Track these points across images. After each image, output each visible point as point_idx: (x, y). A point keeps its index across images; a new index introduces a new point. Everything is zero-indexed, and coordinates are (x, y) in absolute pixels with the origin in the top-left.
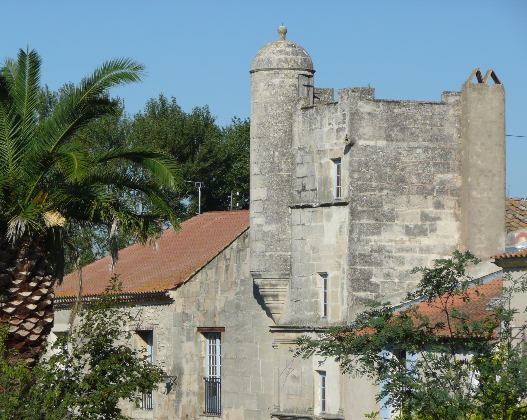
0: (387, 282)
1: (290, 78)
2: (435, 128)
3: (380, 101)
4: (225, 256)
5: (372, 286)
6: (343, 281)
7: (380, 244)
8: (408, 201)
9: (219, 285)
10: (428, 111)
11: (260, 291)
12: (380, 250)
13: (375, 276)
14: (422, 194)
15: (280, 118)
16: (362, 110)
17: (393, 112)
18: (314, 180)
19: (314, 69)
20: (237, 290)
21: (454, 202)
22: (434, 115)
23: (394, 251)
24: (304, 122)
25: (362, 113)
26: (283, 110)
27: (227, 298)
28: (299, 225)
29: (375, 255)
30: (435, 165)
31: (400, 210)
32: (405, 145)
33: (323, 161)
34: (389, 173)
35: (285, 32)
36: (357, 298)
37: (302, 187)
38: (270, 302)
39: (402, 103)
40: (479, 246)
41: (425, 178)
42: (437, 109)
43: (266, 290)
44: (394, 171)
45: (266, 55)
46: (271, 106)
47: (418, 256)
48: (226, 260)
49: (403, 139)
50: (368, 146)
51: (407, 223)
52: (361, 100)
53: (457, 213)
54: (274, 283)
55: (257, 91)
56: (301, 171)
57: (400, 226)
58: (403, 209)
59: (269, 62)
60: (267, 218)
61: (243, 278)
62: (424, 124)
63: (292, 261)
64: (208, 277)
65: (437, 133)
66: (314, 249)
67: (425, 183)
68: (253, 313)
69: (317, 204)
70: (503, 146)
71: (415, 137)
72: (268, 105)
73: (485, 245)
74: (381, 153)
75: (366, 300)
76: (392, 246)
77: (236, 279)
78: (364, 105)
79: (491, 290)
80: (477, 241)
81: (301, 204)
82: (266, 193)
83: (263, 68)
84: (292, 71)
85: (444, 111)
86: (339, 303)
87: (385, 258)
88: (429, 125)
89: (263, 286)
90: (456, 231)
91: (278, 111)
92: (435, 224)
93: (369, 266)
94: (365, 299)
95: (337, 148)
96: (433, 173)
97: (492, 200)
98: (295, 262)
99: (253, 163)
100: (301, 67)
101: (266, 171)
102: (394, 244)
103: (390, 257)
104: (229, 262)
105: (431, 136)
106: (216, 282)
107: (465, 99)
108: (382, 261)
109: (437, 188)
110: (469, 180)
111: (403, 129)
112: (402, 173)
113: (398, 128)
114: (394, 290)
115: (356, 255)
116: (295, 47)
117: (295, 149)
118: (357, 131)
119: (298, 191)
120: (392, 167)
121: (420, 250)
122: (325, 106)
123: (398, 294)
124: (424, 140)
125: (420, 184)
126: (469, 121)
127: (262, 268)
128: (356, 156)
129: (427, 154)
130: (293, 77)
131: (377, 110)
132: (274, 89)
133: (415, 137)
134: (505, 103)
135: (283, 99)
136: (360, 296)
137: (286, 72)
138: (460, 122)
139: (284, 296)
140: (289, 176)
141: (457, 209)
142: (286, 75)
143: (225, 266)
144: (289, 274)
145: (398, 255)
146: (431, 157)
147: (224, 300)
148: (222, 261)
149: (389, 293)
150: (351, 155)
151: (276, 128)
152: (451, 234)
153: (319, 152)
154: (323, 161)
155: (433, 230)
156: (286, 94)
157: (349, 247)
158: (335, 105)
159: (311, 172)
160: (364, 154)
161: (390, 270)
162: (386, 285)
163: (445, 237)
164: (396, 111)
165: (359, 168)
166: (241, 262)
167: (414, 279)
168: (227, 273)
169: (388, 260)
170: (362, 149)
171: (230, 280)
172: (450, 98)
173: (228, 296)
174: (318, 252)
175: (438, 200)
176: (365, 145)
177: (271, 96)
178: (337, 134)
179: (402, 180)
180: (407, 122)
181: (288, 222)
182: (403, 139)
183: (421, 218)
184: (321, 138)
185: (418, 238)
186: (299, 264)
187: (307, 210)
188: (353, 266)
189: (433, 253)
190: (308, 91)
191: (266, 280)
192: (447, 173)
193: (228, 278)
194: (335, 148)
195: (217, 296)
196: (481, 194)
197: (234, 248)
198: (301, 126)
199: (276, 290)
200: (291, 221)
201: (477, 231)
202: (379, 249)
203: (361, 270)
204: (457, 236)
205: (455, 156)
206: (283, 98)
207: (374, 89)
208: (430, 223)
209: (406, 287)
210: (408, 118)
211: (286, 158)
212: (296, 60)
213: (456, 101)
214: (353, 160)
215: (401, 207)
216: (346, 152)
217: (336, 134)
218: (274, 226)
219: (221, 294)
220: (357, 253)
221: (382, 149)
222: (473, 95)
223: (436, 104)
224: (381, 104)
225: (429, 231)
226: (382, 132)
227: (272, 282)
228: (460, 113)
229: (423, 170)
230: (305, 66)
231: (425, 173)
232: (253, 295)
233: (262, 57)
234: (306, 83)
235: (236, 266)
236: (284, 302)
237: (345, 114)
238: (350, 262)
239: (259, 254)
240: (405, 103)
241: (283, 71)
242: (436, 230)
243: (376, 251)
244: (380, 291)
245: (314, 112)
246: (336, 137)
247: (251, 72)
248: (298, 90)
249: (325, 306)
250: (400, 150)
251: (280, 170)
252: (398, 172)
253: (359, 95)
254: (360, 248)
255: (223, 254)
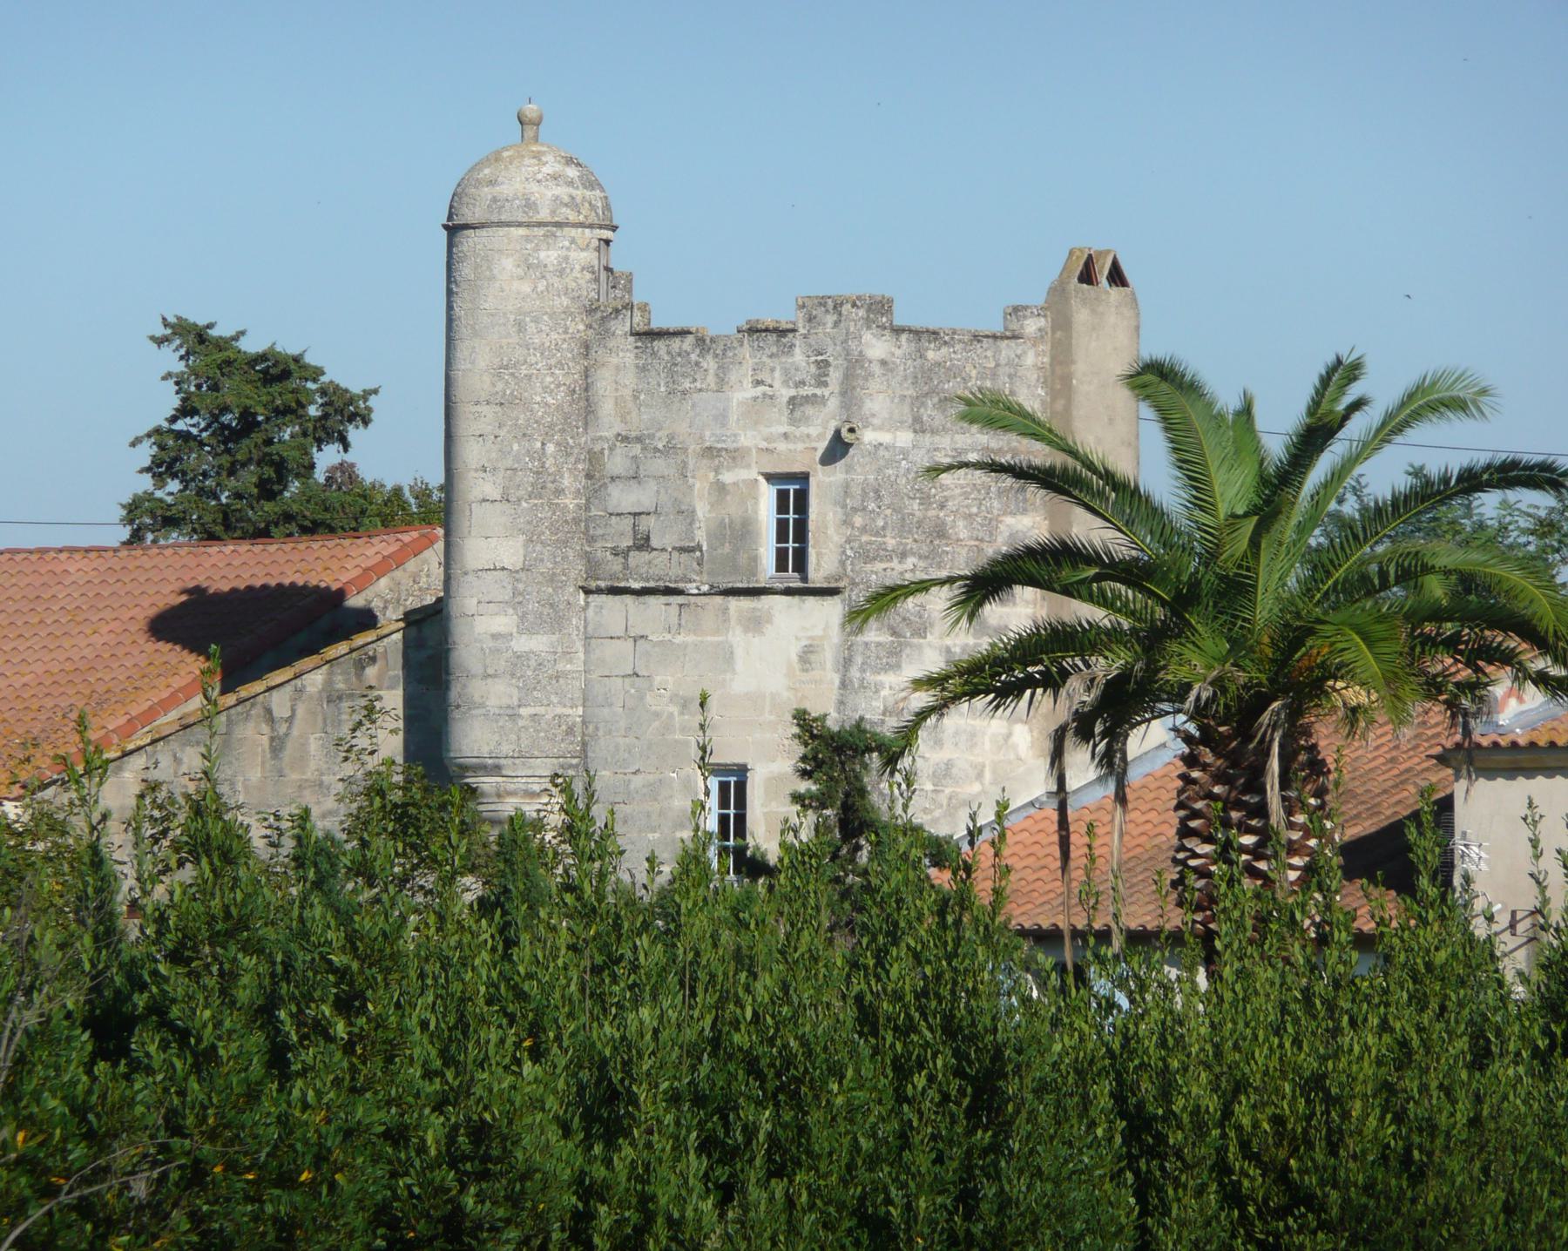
24: (643, 369)
26: (566, 332)
34: (918, 513)
46: (536, 320)
52: (869, 328)
59: (529, 205)
60: (523, 618)
67: (982, 540)
77: (322, 774)
78: (874, 341)
82: (521, 551)
89: (499, 796)
91: (554, 336)
98: (600, 733)
101: (521, 493)
113: (936, 400)
127: (506, 749)
131: (898, 352)
137: (573, 232)
142: (573, 241)
151: (549, 379)
153: (709, 452)
154: (727, 477)
164: (931, 355)
171: (295, 776)
187: (655, 602)
194: (782, 446)
198: (629, 379)
206: (565, 301)
209: (945, 803)
211: (572, 459)
218: (545, 638)
221: (905, 453)
224: (904, 337)
241: (566, 230)
251: (559, 492)
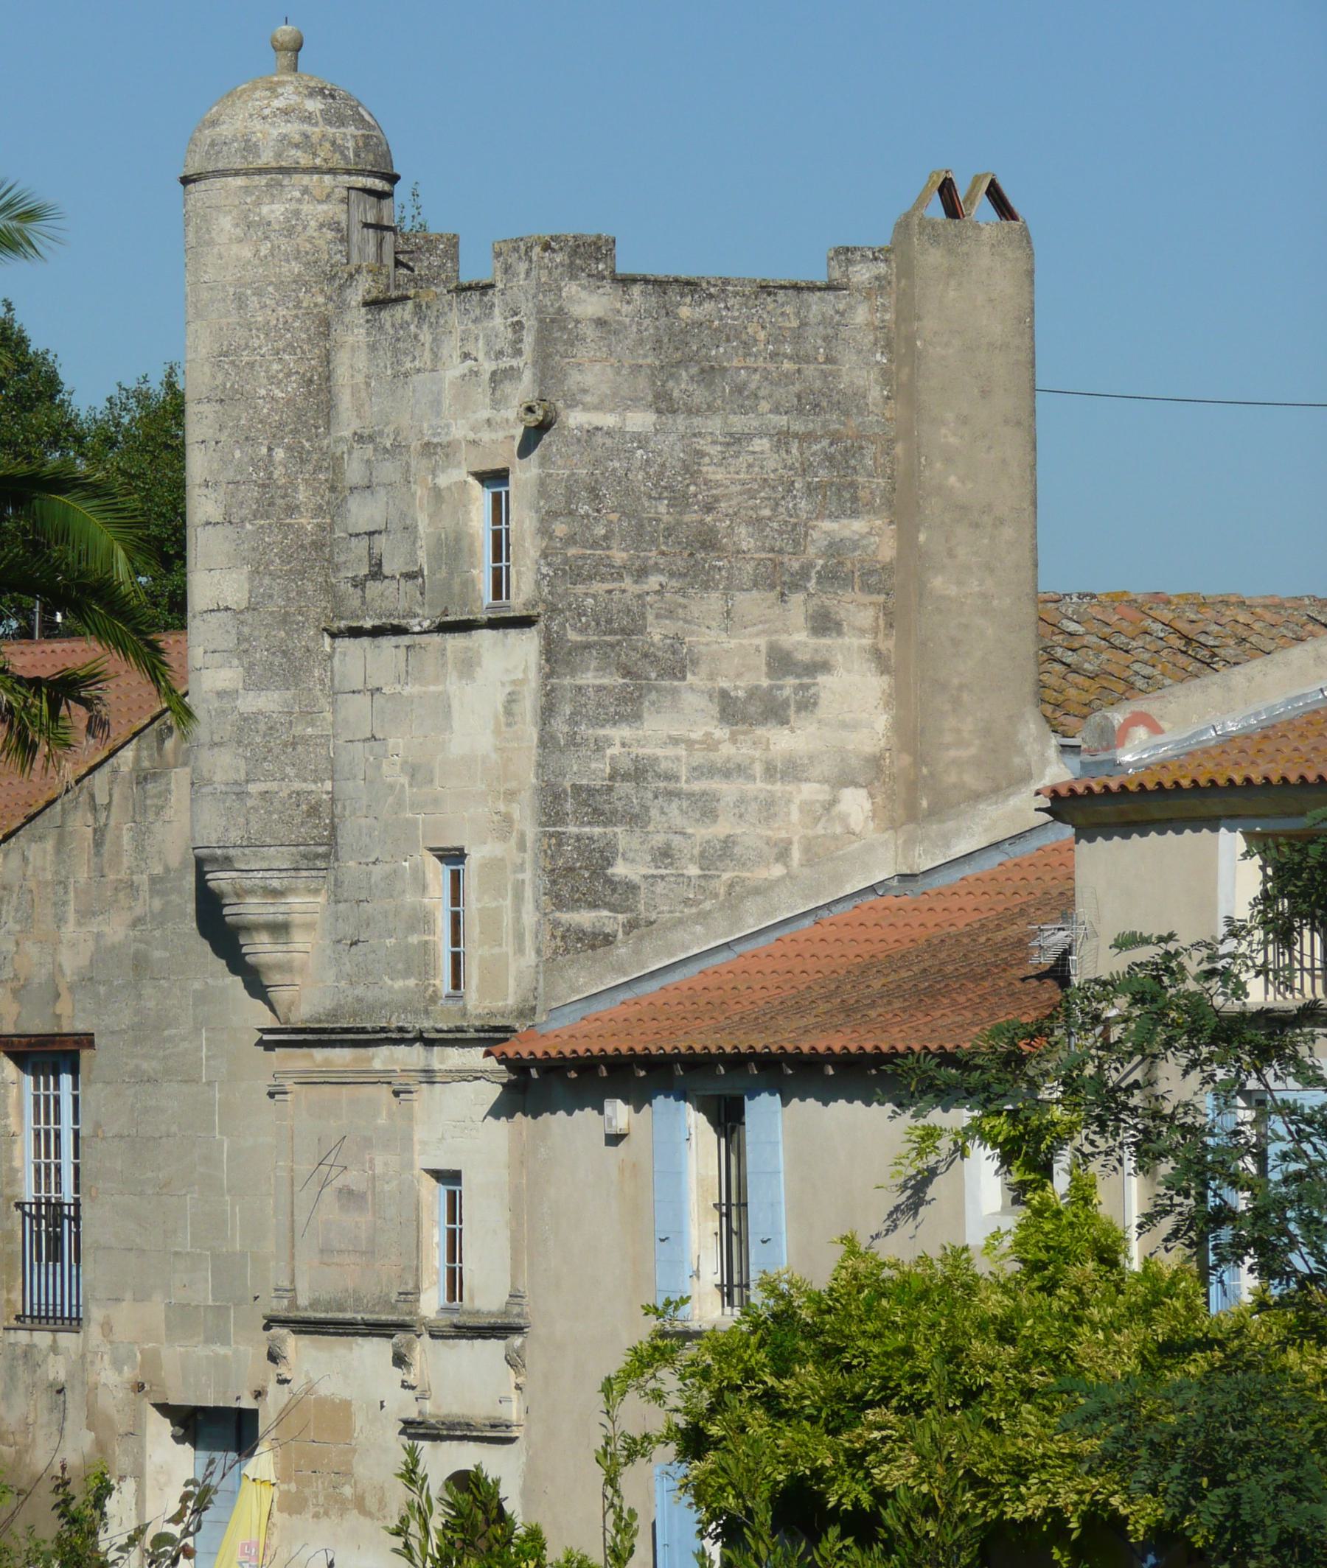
0: (662, 877)
1: (320, 202)
2: (810, 370)
3: (634, 280)
4: (92, 797)
5: (614, 890)
6: (520, 876)
7: (641, 751)
8: (728, 612)
9: (72, 894)
10: (786, 311)
11: (226, 911)
12: (639, 772)
13: (625, 859)
14: (772, 587)
15: (289, 335)
16: (576, 310)
17: (676, 317)
18: (414, 543)
19: (396, 170)
20: (139, 910)
21: (871, 612)
22: (806, 324)
23: (684, 775)
24: (373, 348)
25: (577, 322)
26: (298, 306)
27: (99, 936)
28: (359, 692)
29: (624, 788)
30: (810, 490)
31: (703, 640)
32: (714, 424)
33: (443, 481)
34: (666, 518)
35: (297, 47)
36: (568, 930)
37: (371, 565)
38: (260, 948)
39: (704, 285)
40: (953, 753)
41: (781, 533)
42: (817, 305)
43: (253, 909)
44: (681, 513)
45: (239, 124)
46: (259, 293)
47: (761, 790)
48: (94, 808)
49: (709, 407)
50: (597, 429)
51: (724, 684)
52: (573, 277)
53: (882, 646)
54: (275, 884)
55: (211, 243)
56: (363, 513)
57: (703, 692)
58: (709, 636)
59: (250, 147)
60: (249, 669)
61: (158, 870)
62: (774, 355)
63: (338, 811)
64: (30, 867)
65: (818, 384)
66: (414, 771)
67: (781, 551)
68: (197, 985)
69: (426, 624)
70: (1027, 424)
71: (748, 397)
72: (249, 292)
73: (973, 751)
74: (640, 452)
75: (595, 935)
76: (678, 759)
77: (132, 873)
78: (584, 294)
79: (1001, 897)
80: (948, 738)
81: (368, 624)
82: (246, 586)
83: (229, 166)
84: (327, 178)
85: (837, 312)
86: (509, 948)
87: (656, 797)
88: (791, 358)
89: (238, 895)
90: (881, 706)
91: (282, 311)
92: (814, 684)
93: (605, 825)
94: (594, 933)
95: (494, 436)
96: (804, 516)
97: (995, 602)
98: (347, 813)
99: (200, 486)
100: (356, 164)
101: (245, 512)
102: (684, 753)
103: (670, 794)
104: (108, 817)
105: (799, 398)
106: (61, 882)
107: (907, 270)
108: (647, 809)
109: (818, 568)
110: (922, 538)
111: (709, 374)
112: (708, 519)
113: (694, 370)
114: (686, 902)
115: (565, 791)
116: (333, 97)
117: (341, 439)
118: (562, 382)
119: (354, 578)
120: (675, 498)
121: (767, 770)
122: (449, 297)
123: (699, 914)
124: (777, 408)
125: (763, 555)
126: (919, 343)
127: (234, 836)
128: (560, 462)
129: (784, 455)
130: (328, 196)
131: (626, 309)
132: (267, 238)
133: (748, 397)
134: (1032, 282)
135: (296, 270)
136: (579, 925)
137: (306, 180)
138: (888, 347)
139: (309, 926)
140: (321, 528)
141: (881, 636)
142: (305, 191)
143: (90, 830)
144: (325, 856)
145: (697, 786)
146: (797, 465)
147: (91, 944)
148: (79, 814)
149: (671, 912)
150: (544, 461)
151: (276, 367)
152: (865, 715)
153: (429, 449)
154: (443, 481)
155: (808, 704)
156: (307, 253)
157: (539, 765)
158: (482, 294)
159: (403, 515)
160: (586, 459)
161: (671, 836)
162: (660, 887)
163: (844, 725)
164: (685, 312)
165: (568, 502)
166: (151, 817)
167: (749, 864)
168: (98, 854)
169: (665, 805)
170: (579, 440)
171: (112, 877)
172: (858, 268)
173: (106, 929)
174: (432, 781)
175: (823, 606)
176: (586, 426)
177: (257, 262)
178: (494, 389)
179: (708, 541)
180: (722, 350)
181: (322, 681)
182: (709, 407)
183: (768, 664)
184: (436, 404)
185: (760, 731)
186: (363, 821)
187: (387, 642)
188: (554, 825)
189: (808, 780)
190: (380, 245)
191: (251, 875)
192: (850, 517)
193: (101, 870)
194: (486, 436)
195: (63, 929)
196: (960, 583)
197: (125, 769)
198: (362, 361)
199: (282, 909)
200: (332, 680)
201: (947, 707)
202: (637, 769)
203: (578, 838)
204: (882, 722)
205: (875, 460)
206: (296, 267)
207: (614, 242)
208: (797, 681)
209: (722, 891)
210: (724, 334)
211: (310, 467)
212: (339, 142)
213: (877, 278)
214: (550, 475)
215: (704, 629)
216: (524, 451)
217: (489, 392)
218: (276, 695)
219: (79, 924)
220: (567, 784)
221: (641, 440)
222: (932, 258)
223: (812, 288)
224: (636, 290)
225: (793, 708)
226: (642, 382)
227: (268, 882)
228: (887, 317)
229: (774, 510)
230: (368, 160)
231: (780, 518)
232: (194, 925)
233: (225, 130)
234: (371, 219)
235: (131, 829)
236: (308, 947)
237: (519, 323)
238: (546, 814)
239: (224, 788)
240: (715, 286)
241: (296, 177)
242: (815, 704)
243: (626, 777)
244: (641, 907)
245: (407, 317)
246: (487, 401)
247: (185, 181)
248: (345, 239)
249: (456, 959)
250: (701, 444)
251: (292, 509)
252: (695, 517)
253: (567, 261)
254: (575, 768)
255: (85, 791)
